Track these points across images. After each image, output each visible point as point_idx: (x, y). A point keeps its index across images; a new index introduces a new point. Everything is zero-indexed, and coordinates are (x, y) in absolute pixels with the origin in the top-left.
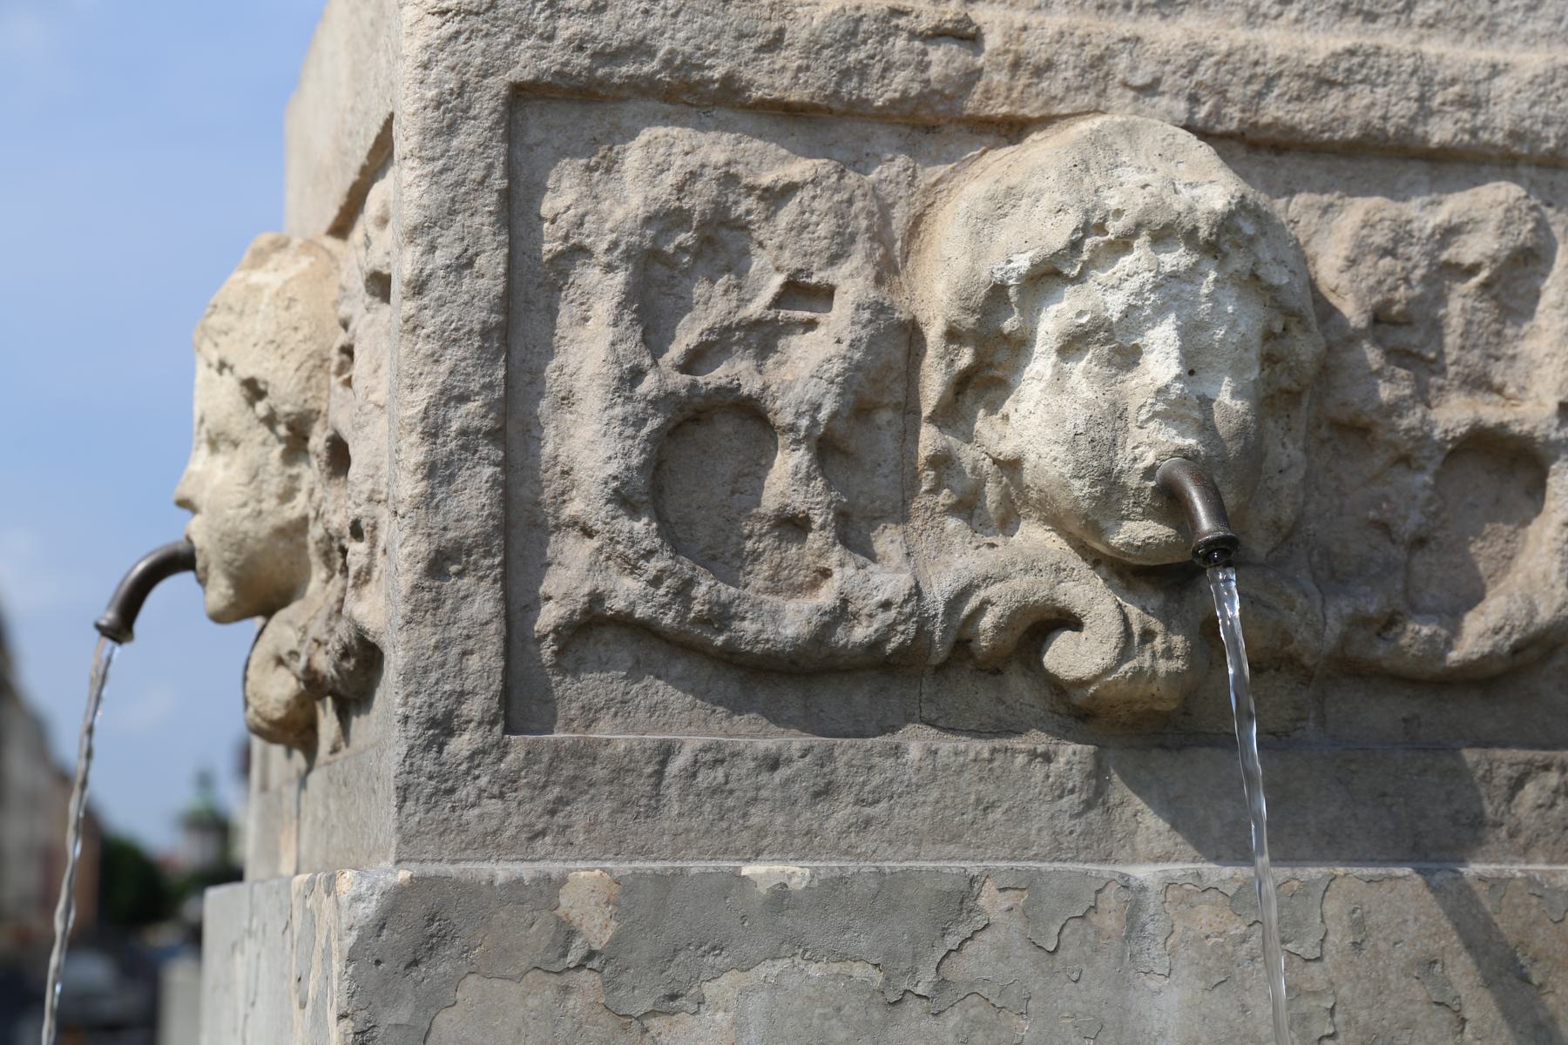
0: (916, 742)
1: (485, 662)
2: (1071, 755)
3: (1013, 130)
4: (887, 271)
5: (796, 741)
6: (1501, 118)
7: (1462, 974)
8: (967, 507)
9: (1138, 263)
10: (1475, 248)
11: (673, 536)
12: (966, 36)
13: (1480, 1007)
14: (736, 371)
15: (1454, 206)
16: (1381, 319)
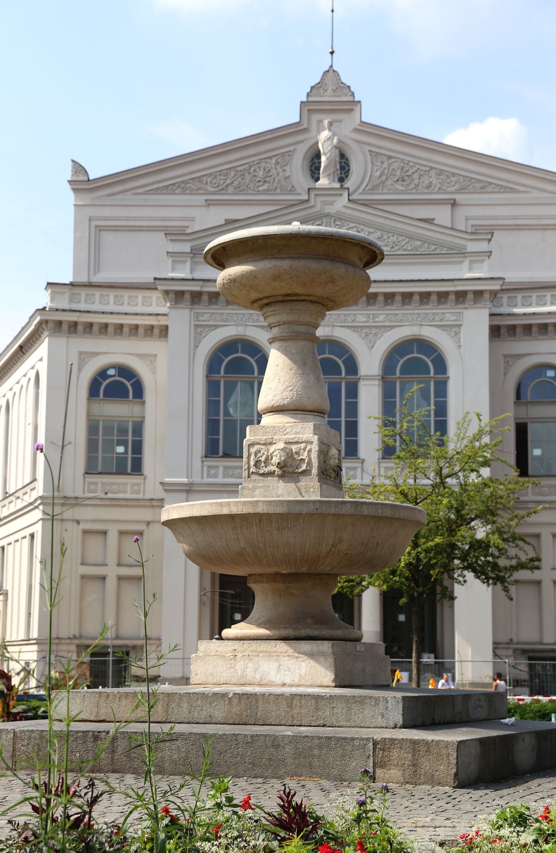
0: (269, 478)
1: (247, 475)
2: (277, 478)
3: (275, 443)
4: (268, 452)
5: (262, 478)
6: (303, 440)
7: (296, 489)
8: (272, 465)
9: (277, 451)
10: (302, 448)
11: (256, 468)
12: (273, 438)
13: (297, 491)
14: (260, 459)
15: (301, 445)
16: (296, 453)
